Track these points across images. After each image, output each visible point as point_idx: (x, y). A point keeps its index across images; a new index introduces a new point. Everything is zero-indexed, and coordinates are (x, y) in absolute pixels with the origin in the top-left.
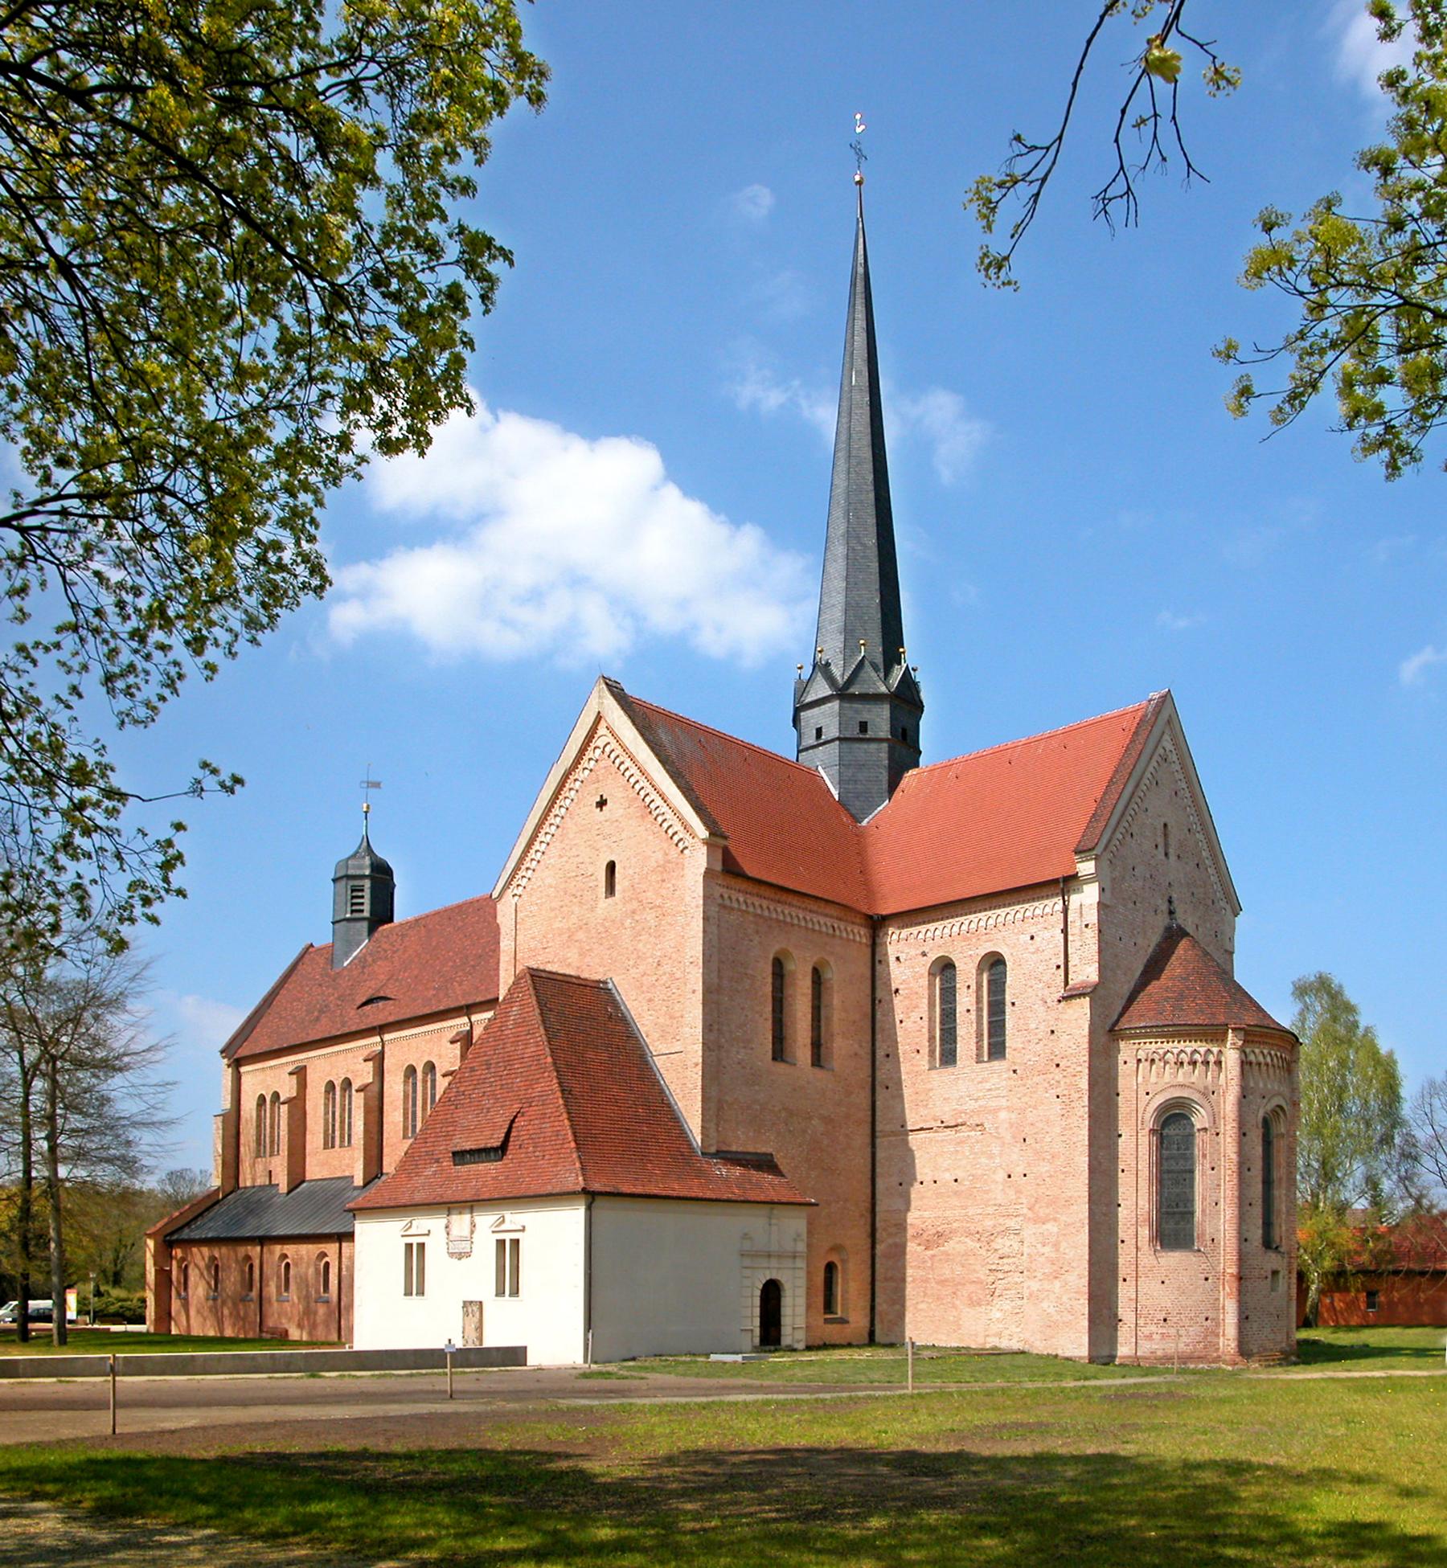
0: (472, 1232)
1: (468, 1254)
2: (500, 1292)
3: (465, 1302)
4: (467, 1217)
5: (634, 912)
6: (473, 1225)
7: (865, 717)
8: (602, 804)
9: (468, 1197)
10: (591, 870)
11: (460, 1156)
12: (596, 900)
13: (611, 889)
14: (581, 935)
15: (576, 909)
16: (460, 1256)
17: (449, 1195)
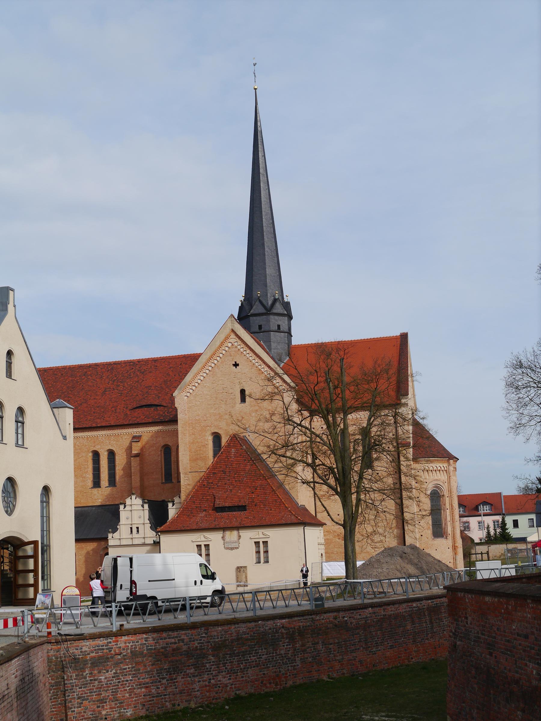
0: (239, 539)
4: (235, 533)
5: (257, 411)
6: (240, 537)
7: (280, 323)
8: (236, 365)
9: (236, 524)
10: (231, 391)
11: (222, 509)
12: (235, 404)
16: (232, 549)
17: (222, 525)
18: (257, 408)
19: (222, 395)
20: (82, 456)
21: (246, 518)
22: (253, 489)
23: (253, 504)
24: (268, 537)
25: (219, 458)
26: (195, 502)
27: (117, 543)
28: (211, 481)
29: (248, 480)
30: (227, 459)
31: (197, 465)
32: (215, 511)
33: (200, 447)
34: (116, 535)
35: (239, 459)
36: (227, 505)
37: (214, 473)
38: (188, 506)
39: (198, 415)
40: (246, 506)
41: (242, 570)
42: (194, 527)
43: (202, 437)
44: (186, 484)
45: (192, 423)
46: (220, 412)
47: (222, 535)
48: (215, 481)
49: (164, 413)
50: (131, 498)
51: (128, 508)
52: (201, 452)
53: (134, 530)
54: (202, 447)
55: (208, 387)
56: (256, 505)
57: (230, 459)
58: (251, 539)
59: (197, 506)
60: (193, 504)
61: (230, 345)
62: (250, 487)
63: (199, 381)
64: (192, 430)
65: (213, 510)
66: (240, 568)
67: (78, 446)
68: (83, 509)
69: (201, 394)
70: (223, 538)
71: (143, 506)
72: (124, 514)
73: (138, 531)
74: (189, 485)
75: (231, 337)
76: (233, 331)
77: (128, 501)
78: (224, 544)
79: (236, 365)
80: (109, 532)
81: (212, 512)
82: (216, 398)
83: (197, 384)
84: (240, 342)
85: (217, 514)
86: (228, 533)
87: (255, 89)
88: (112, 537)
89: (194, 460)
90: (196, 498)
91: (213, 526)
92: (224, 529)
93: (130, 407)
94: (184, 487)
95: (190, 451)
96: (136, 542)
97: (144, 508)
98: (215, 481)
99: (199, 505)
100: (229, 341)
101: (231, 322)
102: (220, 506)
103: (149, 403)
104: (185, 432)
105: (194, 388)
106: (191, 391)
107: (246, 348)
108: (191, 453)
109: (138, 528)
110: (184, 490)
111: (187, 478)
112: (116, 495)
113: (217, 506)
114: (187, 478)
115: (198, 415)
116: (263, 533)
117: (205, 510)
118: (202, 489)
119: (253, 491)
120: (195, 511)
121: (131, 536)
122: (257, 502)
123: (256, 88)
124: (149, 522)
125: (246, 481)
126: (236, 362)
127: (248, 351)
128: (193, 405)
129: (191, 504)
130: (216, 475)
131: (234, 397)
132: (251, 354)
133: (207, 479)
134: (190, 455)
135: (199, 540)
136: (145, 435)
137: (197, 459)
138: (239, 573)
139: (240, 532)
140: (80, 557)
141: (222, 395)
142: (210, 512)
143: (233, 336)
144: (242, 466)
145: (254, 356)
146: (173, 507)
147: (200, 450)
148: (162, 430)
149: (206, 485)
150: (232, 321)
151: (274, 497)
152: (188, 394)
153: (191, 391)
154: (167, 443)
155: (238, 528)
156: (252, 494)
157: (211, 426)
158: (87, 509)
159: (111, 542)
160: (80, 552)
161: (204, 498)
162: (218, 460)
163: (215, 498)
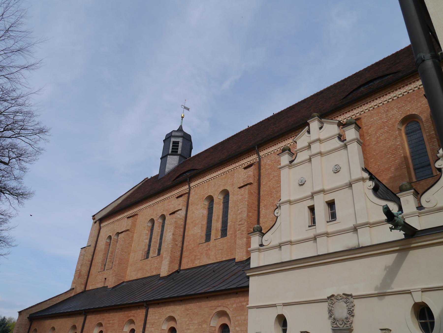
20: (274, 177)
67: (269, 165)
73: (333, 216)
88: (261, 245)
109: (331, 204)
136: (365, 116)
148: (394, 98)
154: (408, 114)
160: (238, 318)
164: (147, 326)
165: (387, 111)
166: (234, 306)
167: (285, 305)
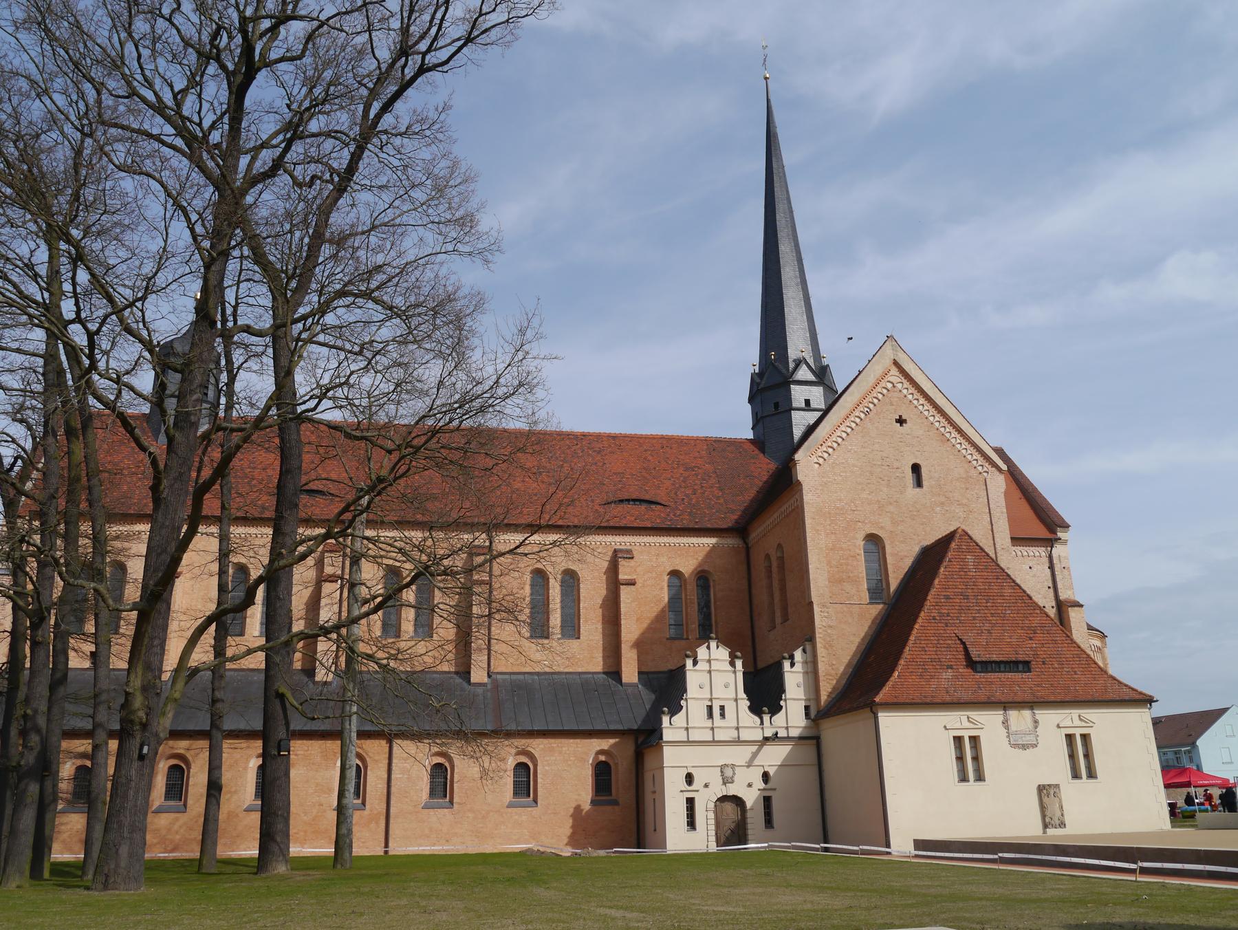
0: (1036, 727)
1: (1034, 746)
2: (1076, 775)
3: (1041, 789)
4: (1027, 713)
5: (942, 503)
6: (1036, 722)
8: (901, 421)
9: (1029, 698)
10: (896, 464)
13: (919, 483)
14: (891, 508)
15: (885, 489)
16: (1024, 747)
17: (998, 696)
18: (943, 499)
19: (880, 470)
21: (1038, 685)
22: (1028, 632)
23: (1037, 660)
24: (1091, 724)
25: (948, 569)
26: (927, 649)
27: (682, 736)
28: (946, 611)
29: (1015, 615)
30: (963, 573)
31: (842, 590)
32: (972, 669)
33: (847, 559)
34: (679, 719)
35: (986, 574)
36: (995, 658)
37: (947, 597)
38: (914, 656)
39: (840, 500)
40: (1030, 662)
41: (1052, 792)
42: (948, 699)
43: (849, 541)
44: (824, 624)
45: (829, 513)
46: (880, 498)
47: (1001, 718)
48: (952, 611)
49: (668, 515)
50: (708, 648)
51: (702, 666)
52: (849, 567)
53: (716, 711)
54: (851, 558)
55: (855, 452)
56: (1044, 663)
57: (969, 573)
58: (1058, 726)
59: (933, 657)
60: (923, 653)
61: (889, 386)
62: (1022, 628)
63: (840, 440)
64: (830, 525)
65: (967, 666)
66: (1048, 787)
68: (514, 677)
69: (843, 463)
70: (1005, 723)
71: (732, 664)
72: (694, 678)
74: (830, 627)
75: (891, 373)
76: (896, 363)
77: (702, 652)
78: (1008, 737)
79: (901, 421)
80: (663, 713)
81: (965, 670)
82: (871, 473)
83: (835, 445)
84: (906, 384)
85: (978, 675)
86: (1013, 714)
87: (766, 78)
89: (836, 580)
90: (926, 642)
91: (983, 698)
92: (1006, 705)
93: (598, 501)
94: (820, 631)
95: (829, 563)
96: (720, 736)
97: (735, 668)
98: (952, 611)
99: (936, 657)
100: (889, 379)
101: (891, 347)
102: (984, 659)
103: (634, 497)
104: (818, 528)
105: (830, 450)
106: (826, 455)
107: (917, 395)
108: (831, 567)
109: (722, 708)
110: (821, 636)
111: (826, 614)
112: (579, 654)
113: (978, 659)
114: (826, 614)
115: (840, 500)
116: (1079, 716)
117: (951, 667)
118: (933, 625)
119: (1031, 636)
120: (931, 667)
121: (709, 723)
122: (1045, 656)
123: (768, 76)
124: (745, 696)
125: (1012, 615)
126: (900, 416)
127: (922, 401)
128: (829, 482)
129: (919, 653)
130: (951, 601)
131: (903, 475)
132: (928, 406)
133: (937, 607)
134: (829, 572)
135: (958, 725)
137: (841, 581)
138: (1046, 797)
139: (1036, 712)
140: (547, 768)
141: (880, 470)
142: (960, 670)
143: (894, 371)
144: (995, 587)
145: (932, 411)
146: (792, 670)
147: (848, 565)
149: (938, 618)
150: (892, 346)
151: (1072, 649)
152: (821, 461)
153: (826, 455)
154: (676, 568)
155: (1031, 705)
156: (1030, 642)
157: (863, 522)
158: (521, 677)
159: (668, 735)
161: (941, 642)
162: (947, 573)
163: (964, 643)
164: (395, 761)
165: (658, 555)
166: (542, 746)
167: (693, 767)
